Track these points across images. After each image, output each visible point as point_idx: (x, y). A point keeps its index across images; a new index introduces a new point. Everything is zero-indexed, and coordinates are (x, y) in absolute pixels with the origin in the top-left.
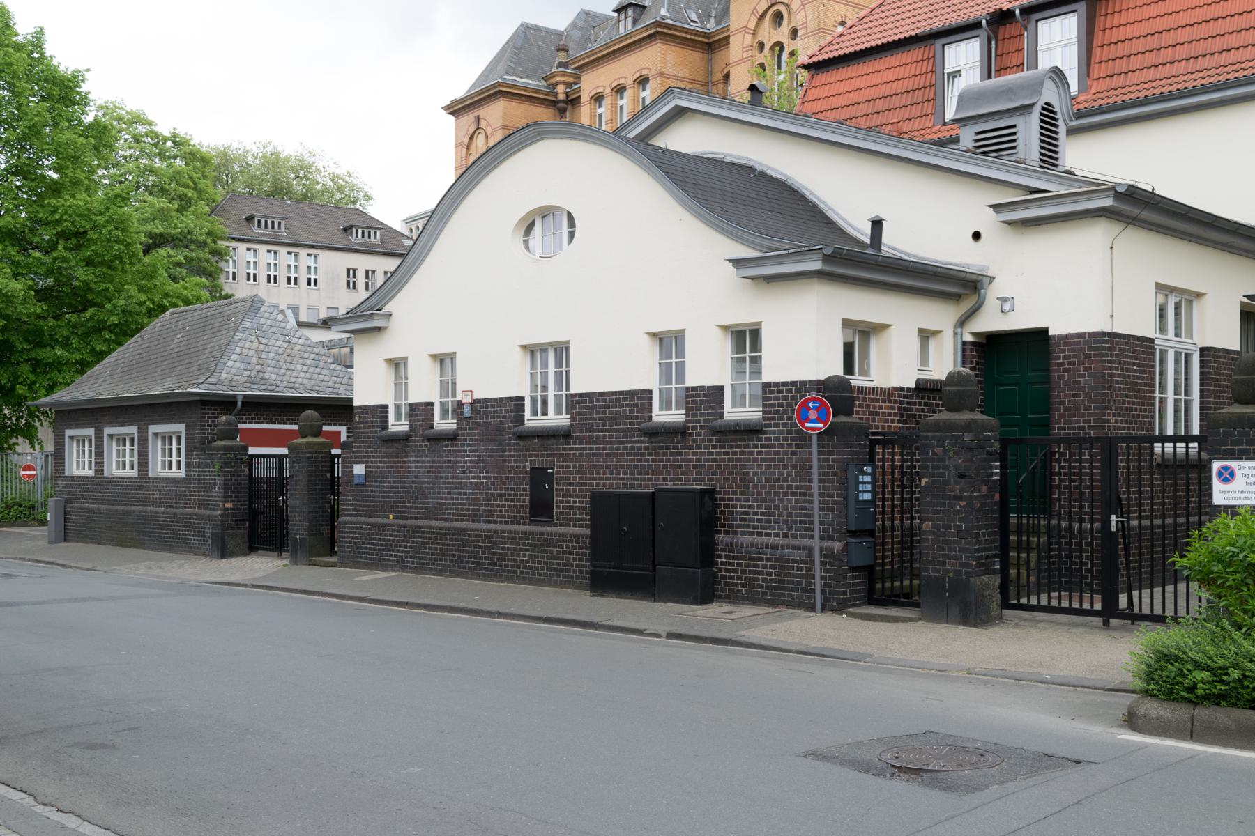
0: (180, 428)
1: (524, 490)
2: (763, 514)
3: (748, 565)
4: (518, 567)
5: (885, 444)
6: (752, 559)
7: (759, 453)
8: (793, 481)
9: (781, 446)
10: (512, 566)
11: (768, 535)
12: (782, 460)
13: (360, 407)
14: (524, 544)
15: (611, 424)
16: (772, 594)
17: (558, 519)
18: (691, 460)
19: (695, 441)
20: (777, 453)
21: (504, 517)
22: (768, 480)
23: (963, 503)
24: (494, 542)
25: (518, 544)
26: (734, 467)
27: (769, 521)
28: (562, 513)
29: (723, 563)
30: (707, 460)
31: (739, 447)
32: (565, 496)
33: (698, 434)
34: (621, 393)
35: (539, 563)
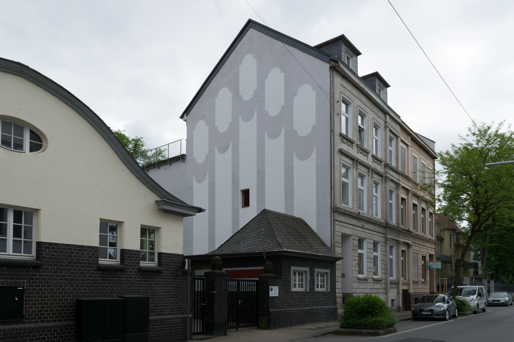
2: (161, 306)
3: (158, 328)
5: (198, 279)
7: (160, 281)
8: (173, 292)
9: (169, 279)
11: (163, 314)
12: (169, 284)
18: (127, 284)
19: (129, 275)
20: (167, 281)
22: (163, 292)
26: (148, 287)
27: (164, 309)
30: (135, 284)
33: (130, 272)
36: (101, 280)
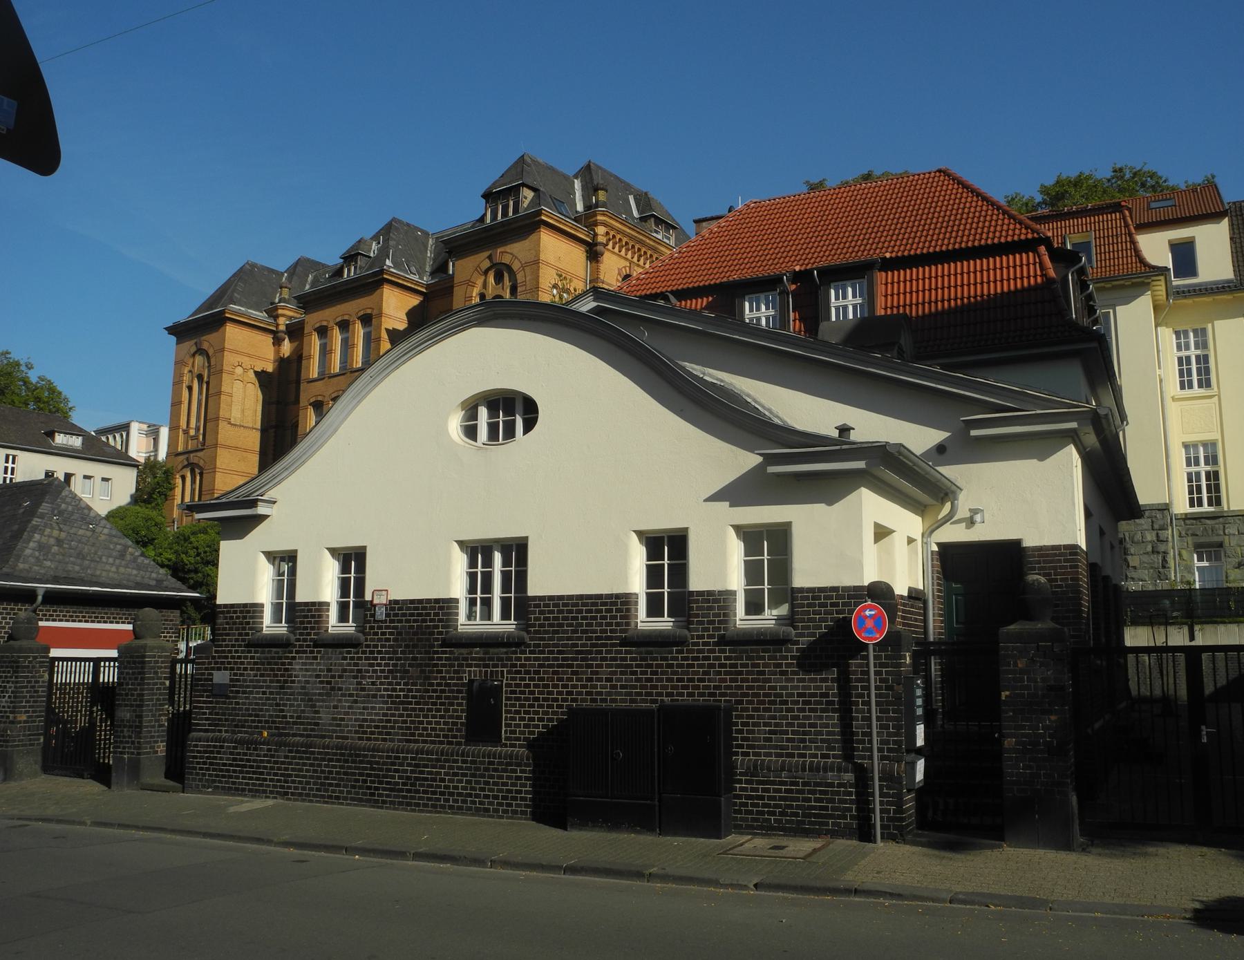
1: (460, 704)
4: (452, 794)
6: (784, 783)
10: (442, 794)
13: (225, 606)
14: (459, 768)
15: (583, 632)
16: (810, 823)
17: (507, 739)
21: (429, 735)
23: (1053, 718)
24: (417, 766)
25: (451, 768)
27: (804, 741)
28: (514, 732)
29: (742, 789)
31: (763, 658)
32: (518, 712)
34: (599, 596)
35: (483, 789)
36: (637, 666)
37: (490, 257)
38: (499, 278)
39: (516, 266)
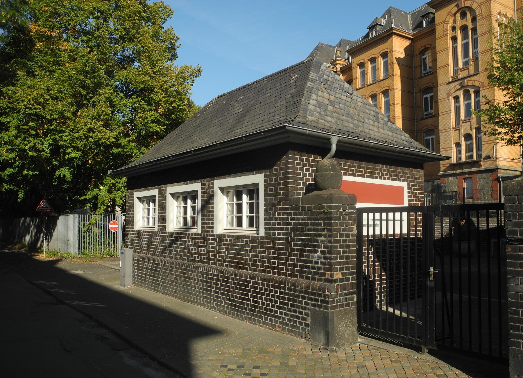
0: (258, 178)
37: (457, 6)
38: (463, 15)
39: (474, 7)
